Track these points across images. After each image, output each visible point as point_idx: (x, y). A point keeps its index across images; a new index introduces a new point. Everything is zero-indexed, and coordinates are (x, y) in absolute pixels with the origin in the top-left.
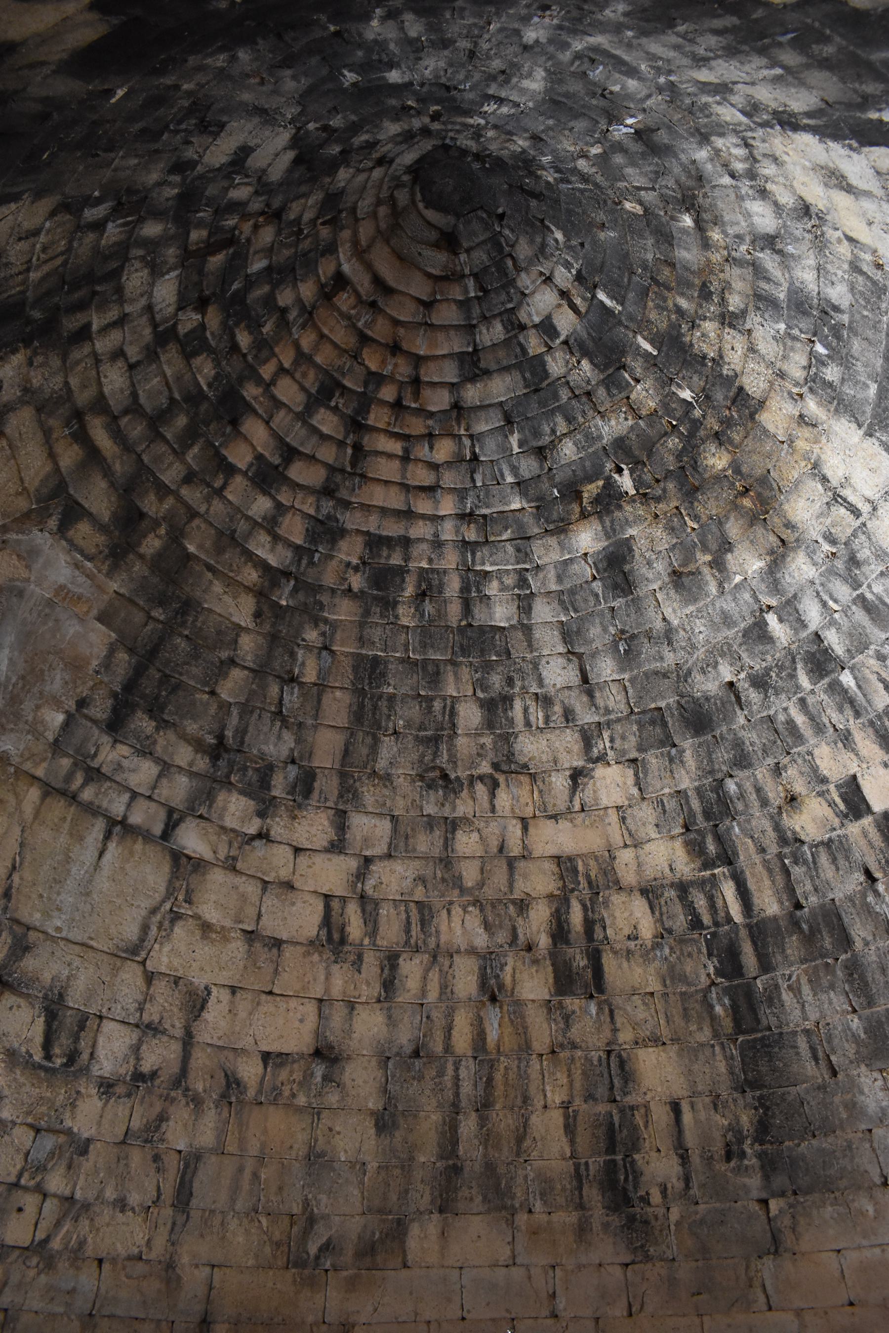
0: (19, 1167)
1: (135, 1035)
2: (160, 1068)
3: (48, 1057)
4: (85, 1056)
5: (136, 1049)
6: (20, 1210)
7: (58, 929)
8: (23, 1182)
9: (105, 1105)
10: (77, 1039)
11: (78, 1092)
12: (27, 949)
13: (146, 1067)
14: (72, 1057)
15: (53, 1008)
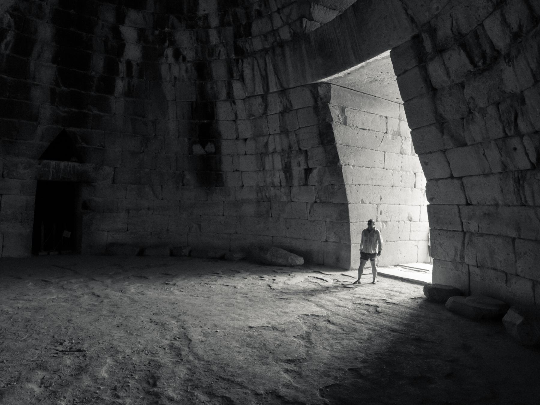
0: (501, 127)
1: (498, 14)
2: (520, 20)
3: (475, 66)
4: (488, 51)
5: (505, 22)
6: (515, 149)
7: (437, 8)
8: (509, 134)
9: (514, 67)
10: (480, 45)
11: (501, 70)
12: (435, 30)
13: (515, 27)
14: (484, 56)
15: (461, 41)
